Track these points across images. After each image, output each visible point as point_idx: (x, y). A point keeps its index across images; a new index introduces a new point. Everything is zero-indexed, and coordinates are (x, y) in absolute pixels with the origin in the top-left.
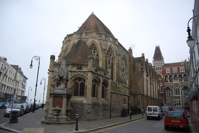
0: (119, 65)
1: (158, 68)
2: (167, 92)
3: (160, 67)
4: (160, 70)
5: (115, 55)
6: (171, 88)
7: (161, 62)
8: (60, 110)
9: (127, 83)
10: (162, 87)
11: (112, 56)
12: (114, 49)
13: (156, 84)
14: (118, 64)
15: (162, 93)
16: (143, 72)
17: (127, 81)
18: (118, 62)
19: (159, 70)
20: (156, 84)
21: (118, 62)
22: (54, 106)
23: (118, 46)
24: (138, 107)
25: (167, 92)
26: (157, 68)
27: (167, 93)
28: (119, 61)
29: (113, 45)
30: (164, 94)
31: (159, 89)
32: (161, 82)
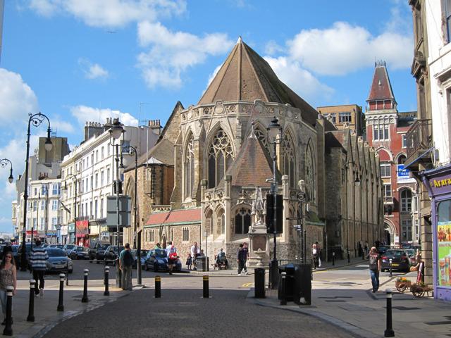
0: (304, 166)
1: (381, 131)
2: (404, 201)
3: (386, 131)
4: (386, 137)
5: (296, 145)
6: (415, 192)
7: (388, 115)
8: (264, 253)
9: (315, 197)
10: (388, 187)
11: (292, 147)
12: (295, 132)
13: (375, 186)
14: (303, 162)
15: (390, 206)
16: (347, 168)
17: (315, 192)
18: (302, 159)
19: (381, 138)
20: (375, 186)
21: (302, 159)
22: (255, 249)
23: (301, 126)
24: (336, 246)
25: (404, 201)
26: (376, 132)
27: (404, 205)
28: (304, 158)
29: (292, 124)
30: (393, 207)
31: (380, 196)
32: (388, 174)
